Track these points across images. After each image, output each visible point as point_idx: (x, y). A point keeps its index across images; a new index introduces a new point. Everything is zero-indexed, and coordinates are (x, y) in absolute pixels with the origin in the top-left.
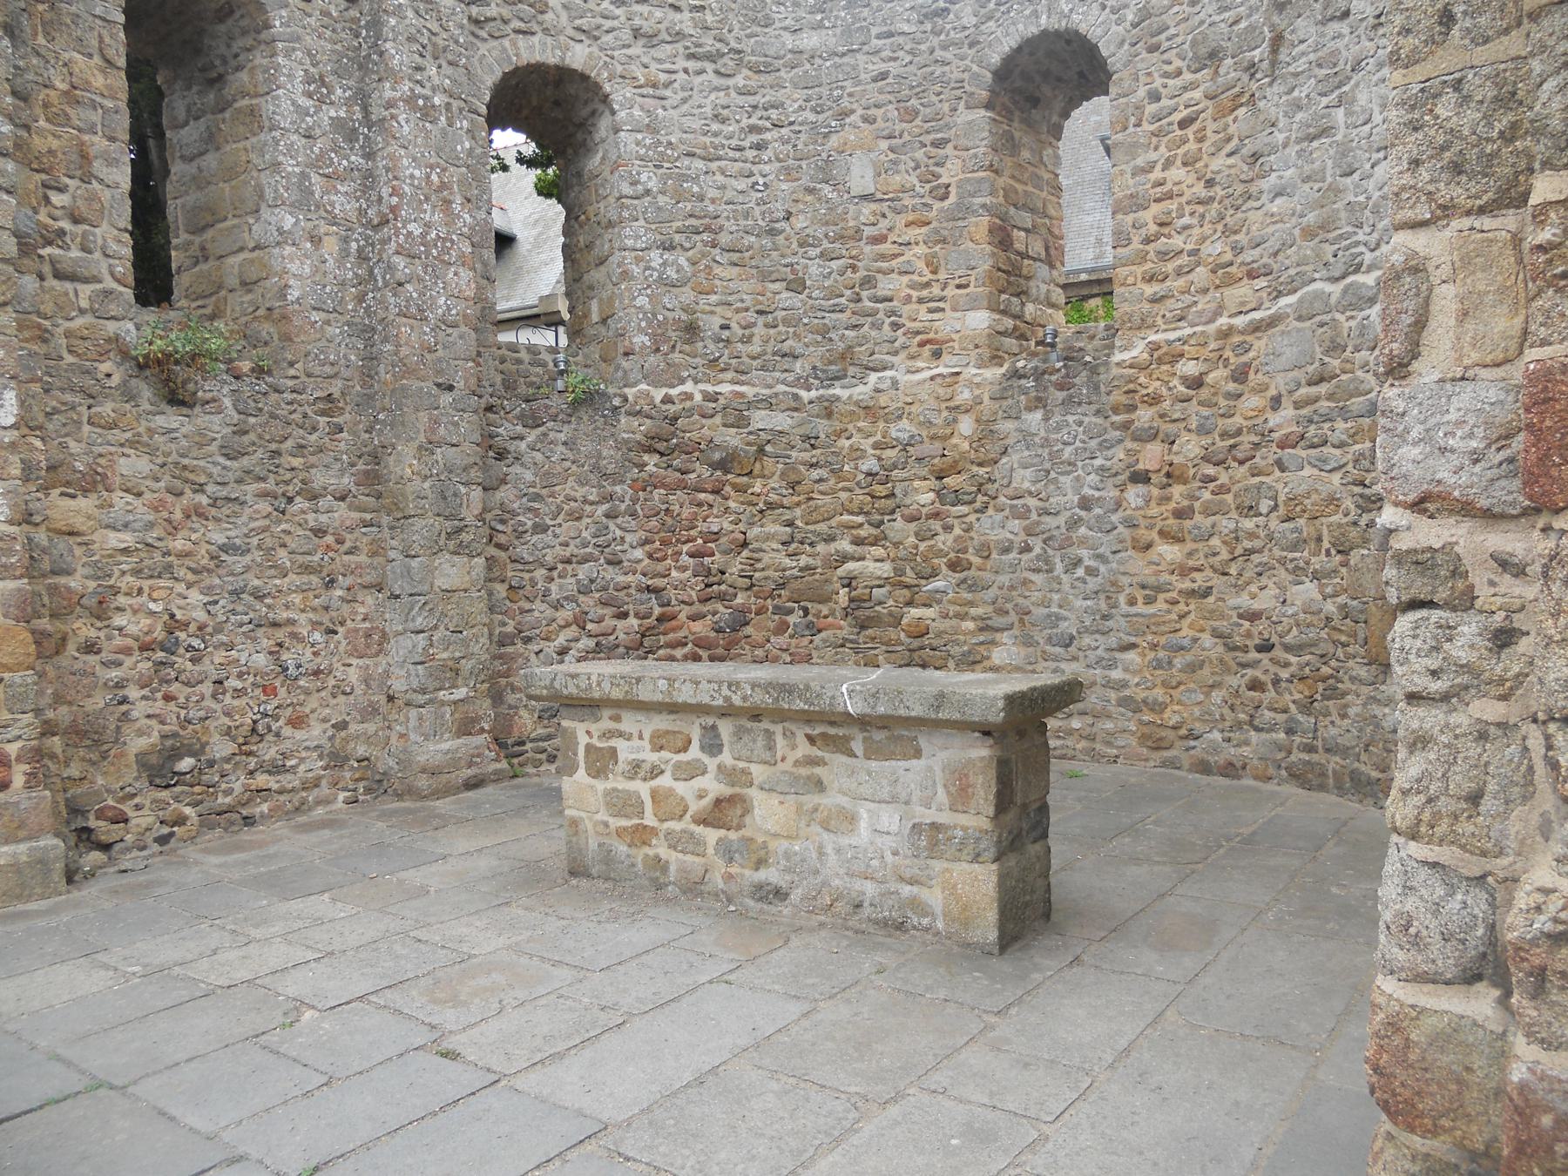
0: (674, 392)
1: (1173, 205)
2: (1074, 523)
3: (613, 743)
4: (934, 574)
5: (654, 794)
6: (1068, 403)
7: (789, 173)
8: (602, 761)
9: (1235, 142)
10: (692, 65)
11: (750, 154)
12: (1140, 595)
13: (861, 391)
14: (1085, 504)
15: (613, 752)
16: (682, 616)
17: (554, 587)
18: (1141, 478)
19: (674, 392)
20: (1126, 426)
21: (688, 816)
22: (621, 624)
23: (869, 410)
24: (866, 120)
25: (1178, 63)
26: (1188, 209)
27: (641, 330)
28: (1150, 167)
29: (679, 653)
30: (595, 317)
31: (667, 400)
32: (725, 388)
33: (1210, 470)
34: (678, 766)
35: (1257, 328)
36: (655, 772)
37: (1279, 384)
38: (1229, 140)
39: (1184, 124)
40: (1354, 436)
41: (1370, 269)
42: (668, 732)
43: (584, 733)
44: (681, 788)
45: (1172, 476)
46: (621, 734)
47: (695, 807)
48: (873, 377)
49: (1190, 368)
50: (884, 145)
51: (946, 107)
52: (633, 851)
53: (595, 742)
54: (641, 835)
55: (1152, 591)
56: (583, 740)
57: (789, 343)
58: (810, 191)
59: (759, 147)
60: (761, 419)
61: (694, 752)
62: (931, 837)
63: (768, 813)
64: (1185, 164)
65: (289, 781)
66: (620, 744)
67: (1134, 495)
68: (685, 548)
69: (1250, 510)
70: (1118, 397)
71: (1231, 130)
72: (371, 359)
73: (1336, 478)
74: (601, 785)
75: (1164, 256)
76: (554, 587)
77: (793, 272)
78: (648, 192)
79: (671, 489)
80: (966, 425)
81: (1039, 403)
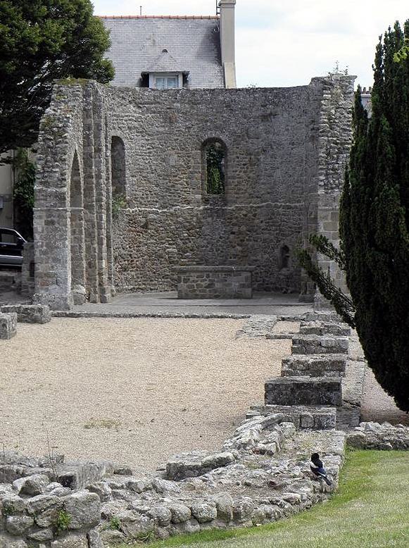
2: (218, 241)
4: (187, 252)
6: (218, 217)
8: (186, 281)
10: (138, 134)
15: (189, 279)
18: (233, 233)
28: (236, 171)
32: (143, 209)
35: (259, 207)
37: (262, 219)
39: (244, 165)
40: (276, 230)
45: (240, 233)
48: (174, 208)
49: (245, 213)
55: (235, 256)
56: (183, 278)
59: (150, 153)
60: (151, 216)
61: (205, 277)
62: (243, 286)
63: (218, 285)
67: (232, 236)
69: (257, 241)
80: (195, 219)
81: (211, 216)
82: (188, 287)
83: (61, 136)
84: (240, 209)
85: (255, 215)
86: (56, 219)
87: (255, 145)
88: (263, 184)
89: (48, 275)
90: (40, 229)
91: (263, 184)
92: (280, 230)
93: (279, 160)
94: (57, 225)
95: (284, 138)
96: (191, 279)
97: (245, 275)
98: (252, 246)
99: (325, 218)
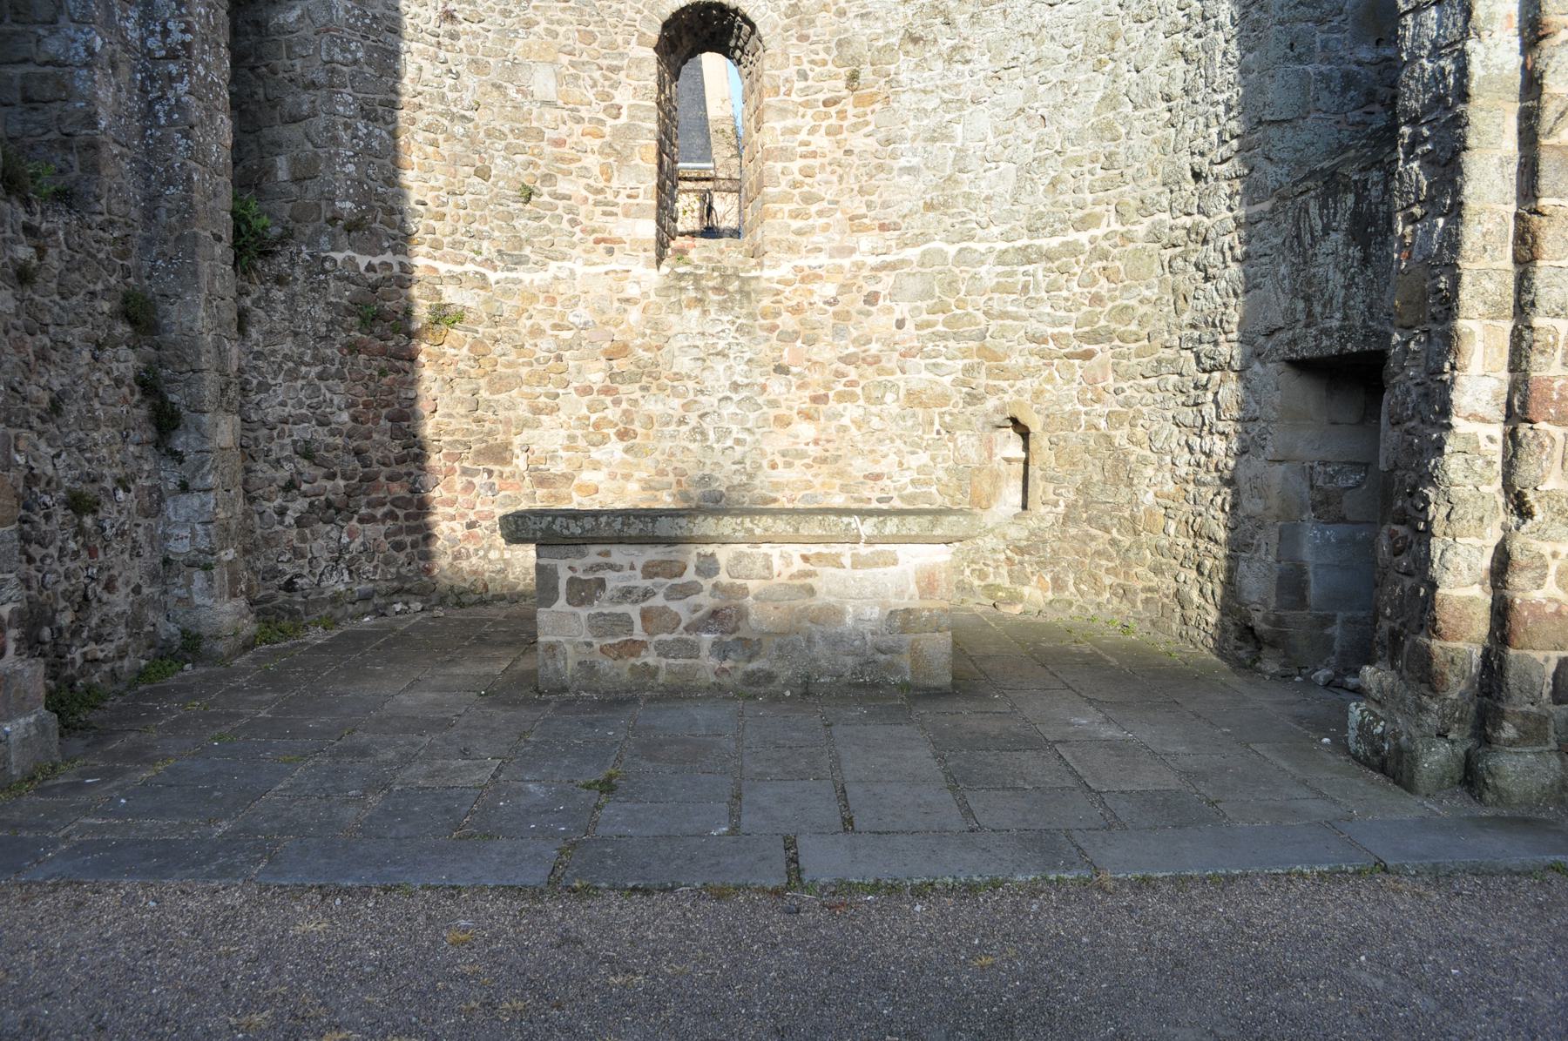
0: (376, 261)
1: (816, 162)
3: (600, 574)
5: (645, 615)
7: (477, 66)
9: (871, 128)
11: (446, 41)
12: (779, 460)
14: (735, 387)
15: (601, 584)
16: (382, 479)
17: (274, 446)
19: (376, 261)
20: (773, 328)
21: (681, 628)
22: (329, 484)
24: (549, 32)
25: (822, 55)
26: (828, 169)
27: (348, 197)
29: (379, 512)
30: (283, 174)
31: (370, 268)
33: (842, 367)
34: (673, 587)
36: (647, 594)
38: (867, 124)
39: (825, 104)
41: (980, 240)
42: (663, 562)
44: (674, 606)
46: (611, 567)
47: (686, 619)
48: (553, 265)
50: (565, 59)
51: (620, 39)
52: (619, 662)
53: (580, 575)
54: (634, 647)
57: (475, 225)
58: (498, 87)
64: (828, 134)
65: (110, 649)
66: (609, 575)
68: (384, 412)
70: (766, 301)
71: (869, 118)
72: (152, 199)
73: (947, 380)
74: (583, 612)
75: (808, 199)
76: (274, 446)
77: (482, 159)
78: (356, 62)
79: (372, 355)
80: (634, 315)
82: (603, 625)
84: (810, 277)
85: (872, 299)
88: (908, 170)
91: (908, 170)
92: (986, 353)
93: (982, 63)
96: (614, 581)
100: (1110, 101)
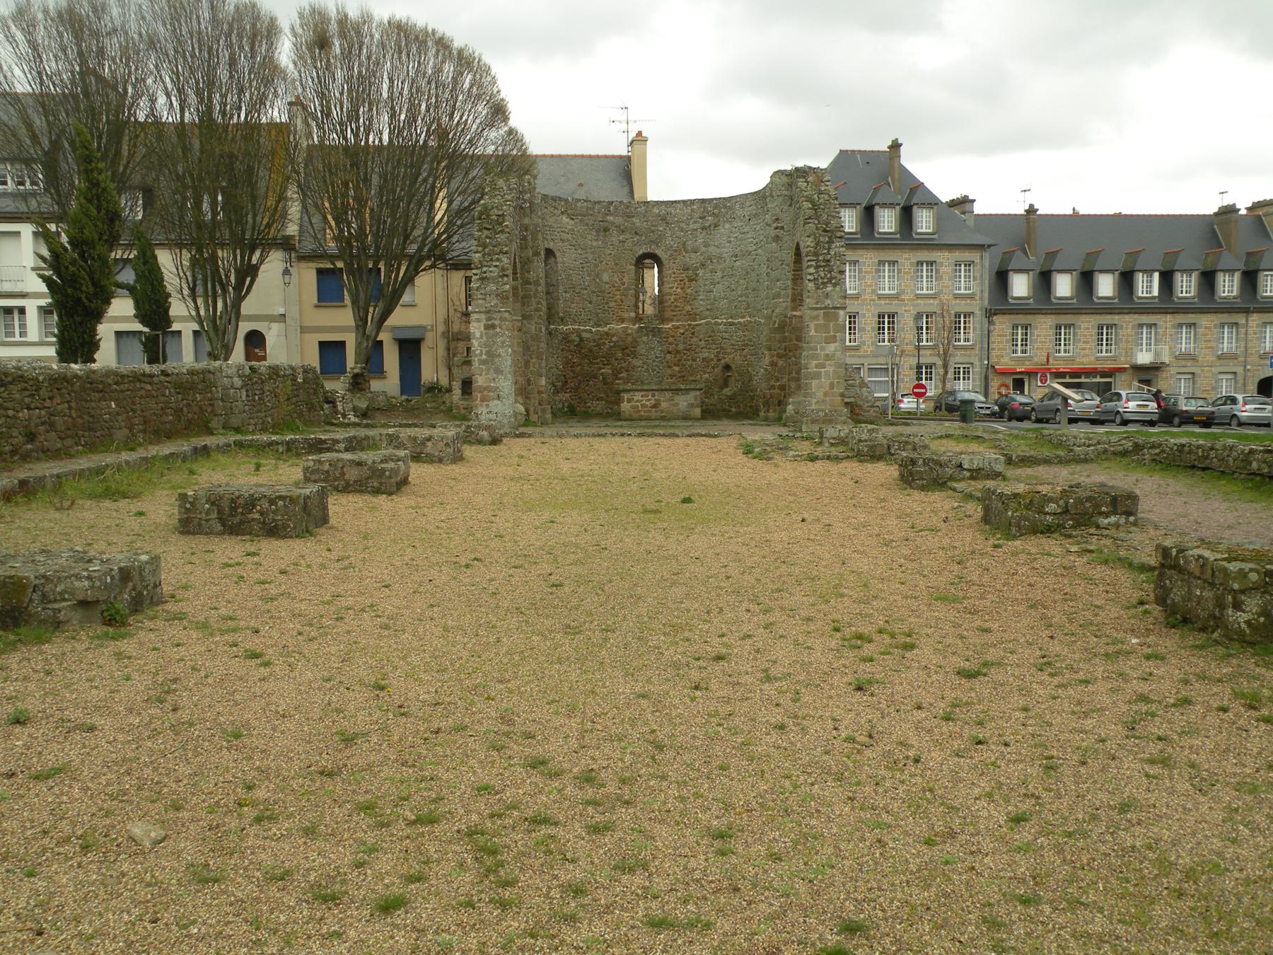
8: (629, 401)
13: (606, 329)
23: (607, 334)
43: (626, 396)
45: (678, 352)
62: (691, 405)
63: (664, 405)
67: (668, 356)
80: (630, 339)
83: (500, 224)
86: (497, 323)
87: (693, 259)
89: (488, 389)
90: (478, 335)
92: (722, 348)
94: (498, 330)
95: (727, 251)
97: (693, 394)
98: (691, 366)
99: (816, 318)
100: (747, 288)
